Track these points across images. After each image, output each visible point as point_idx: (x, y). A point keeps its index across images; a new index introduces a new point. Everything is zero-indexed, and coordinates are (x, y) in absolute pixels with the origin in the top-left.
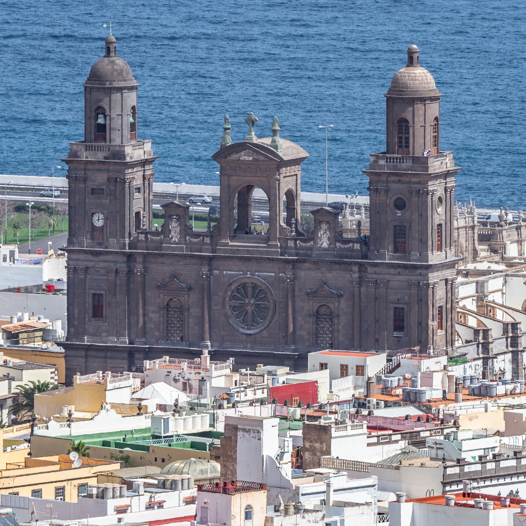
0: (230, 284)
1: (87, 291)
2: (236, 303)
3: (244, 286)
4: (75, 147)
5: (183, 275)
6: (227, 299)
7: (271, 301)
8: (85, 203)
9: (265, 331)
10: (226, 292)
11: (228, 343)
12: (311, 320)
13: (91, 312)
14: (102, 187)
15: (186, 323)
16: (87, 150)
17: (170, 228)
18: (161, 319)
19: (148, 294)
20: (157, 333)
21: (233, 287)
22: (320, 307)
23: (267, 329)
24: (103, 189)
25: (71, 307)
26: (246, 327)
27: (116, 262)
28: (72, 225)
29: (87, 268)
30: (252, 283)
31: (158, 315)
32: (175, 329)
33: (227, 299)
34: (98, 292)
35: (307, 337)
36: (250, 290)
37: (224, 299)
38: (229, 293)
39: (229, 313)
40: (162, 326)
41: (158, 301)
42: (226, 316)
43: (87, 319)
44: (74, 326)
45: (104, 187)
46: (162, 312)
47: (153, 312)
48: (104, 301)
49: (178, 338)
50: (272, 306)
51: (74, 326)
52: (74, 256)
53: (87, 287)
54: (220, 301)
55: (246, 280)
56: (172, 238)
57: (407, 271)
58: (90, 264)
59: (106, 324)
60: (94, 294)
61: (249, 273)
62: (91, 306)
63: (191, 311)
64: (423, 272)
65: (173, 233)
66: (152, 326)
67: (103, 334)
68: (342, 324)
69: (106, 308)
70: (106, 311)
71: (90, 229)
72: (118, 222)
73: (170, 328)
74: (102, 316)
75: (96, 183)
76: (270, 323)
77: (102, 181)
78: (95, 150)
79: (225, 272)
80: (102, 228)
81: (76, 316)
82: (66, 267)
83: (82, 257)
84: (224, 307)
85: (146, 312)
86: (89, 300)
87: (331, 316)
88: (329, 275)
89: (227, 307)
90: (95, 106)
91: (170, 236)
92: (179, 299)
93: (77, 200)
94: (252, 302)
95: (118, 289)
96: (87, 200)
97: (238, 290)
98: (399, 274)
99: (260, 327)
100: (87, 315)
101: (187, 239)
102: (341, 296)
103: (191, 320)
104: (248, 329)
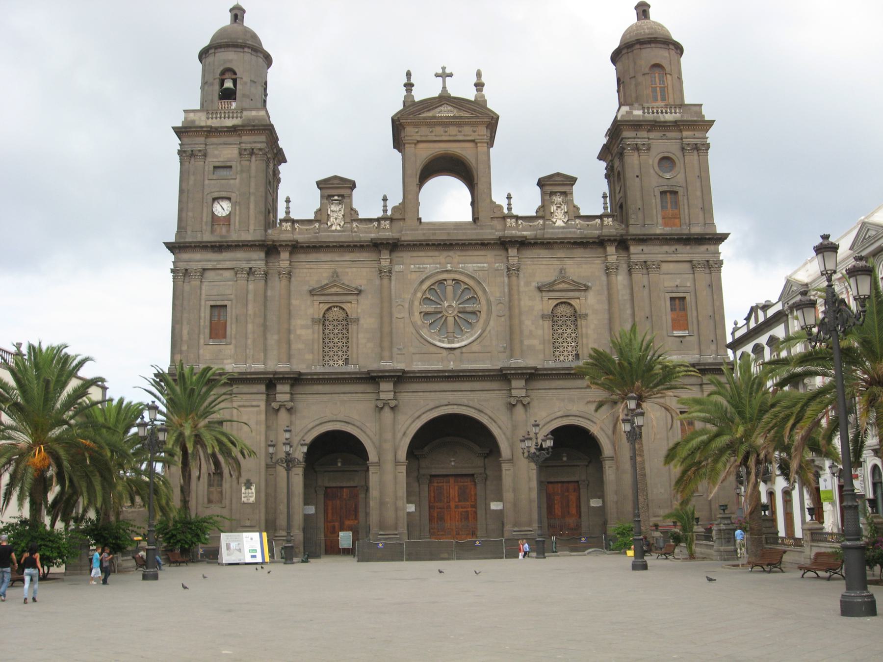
0: (422, 282)
1: (203, 303)
2: (430, 308)
3: (441, 282)
4: (192, 115)
5: (350, 274)
6: (417, 303)
7: (483, 302)
8: (203, 185)
9: (475, 343)
10: (415, 292)
11: (420, 363)
12: (547, 324)
13: (207, 331)
14: (229, 164)
15: (354, 340)
16: (208, 118)
17: (329, 213)
18: (316, 336)
19: (294, 302)
20: (309, 357)
21: (425, 286)
22: (557, 304)
23: (478, 341)
24: (231, 167)
25: (178, 327)
26: (446, 339)
27: (249, 260)
28: (184, 215)
29: (204, 270)
30: (454, 280)
31: (310, 331)
32: (336, 349)
33: (417, 303)
34: (219, 303)
35: (541, 347)
36: (449, 289)
37: (411, 303)
38: (419, 295)
39: (419, 323)
40: (316, 346)
41: (310, 311)
42: (414, 325)
43: (202, 341)
44: (181, 352)
45: (233, 164)
46: (316, 328)
47: (303, 327)
48: (229, 314)
49: (340, 362)
50: (484, 309)
51: (181, 352)
52: (185, 256)
53: (203, 296)
54: (407, 306)
55: (444, 276)
56: (332, 225)
57: (688, 247)
58: (209, 265)
59: (231, 347)
60: (212, 306)
61: (449, 265)
62: (208, 323)
63: (362, 321)
64: (711, 248)
65: (332, 219)
66: (301, 346)
67: (225, 361)
68: (592, 326)
69: (231, 324)
70: (231, 329)
71: (210, 219)
72: (252, 206)
73: (327, 349)
74: (225, 337)
75: (221, 159)
76: (483, 331)
77: (229, 156)
78: (220, 118)
79: (412, 266)
80: (228, 218)
81: (185, 336)
82: (173, 271)
83: (198, 256)
84: (411, 313)
85: (292, 328)
86: (205, 313)
87: (576, 317)
88: (568, 262)
89: (417, 314)
90: (222, 68)
91: (329, 224)
92: (341, 308)
93: (191, 182)
94: (454, 305)
95: (251, 297)
96: (207, 182)
97: (430, 289)
98: (675, 252)
99: (467, 338)
100: (202, 336)
101: (354, 226)
102: (587, 289)
103: (361, 336)
104: (449, 343)
